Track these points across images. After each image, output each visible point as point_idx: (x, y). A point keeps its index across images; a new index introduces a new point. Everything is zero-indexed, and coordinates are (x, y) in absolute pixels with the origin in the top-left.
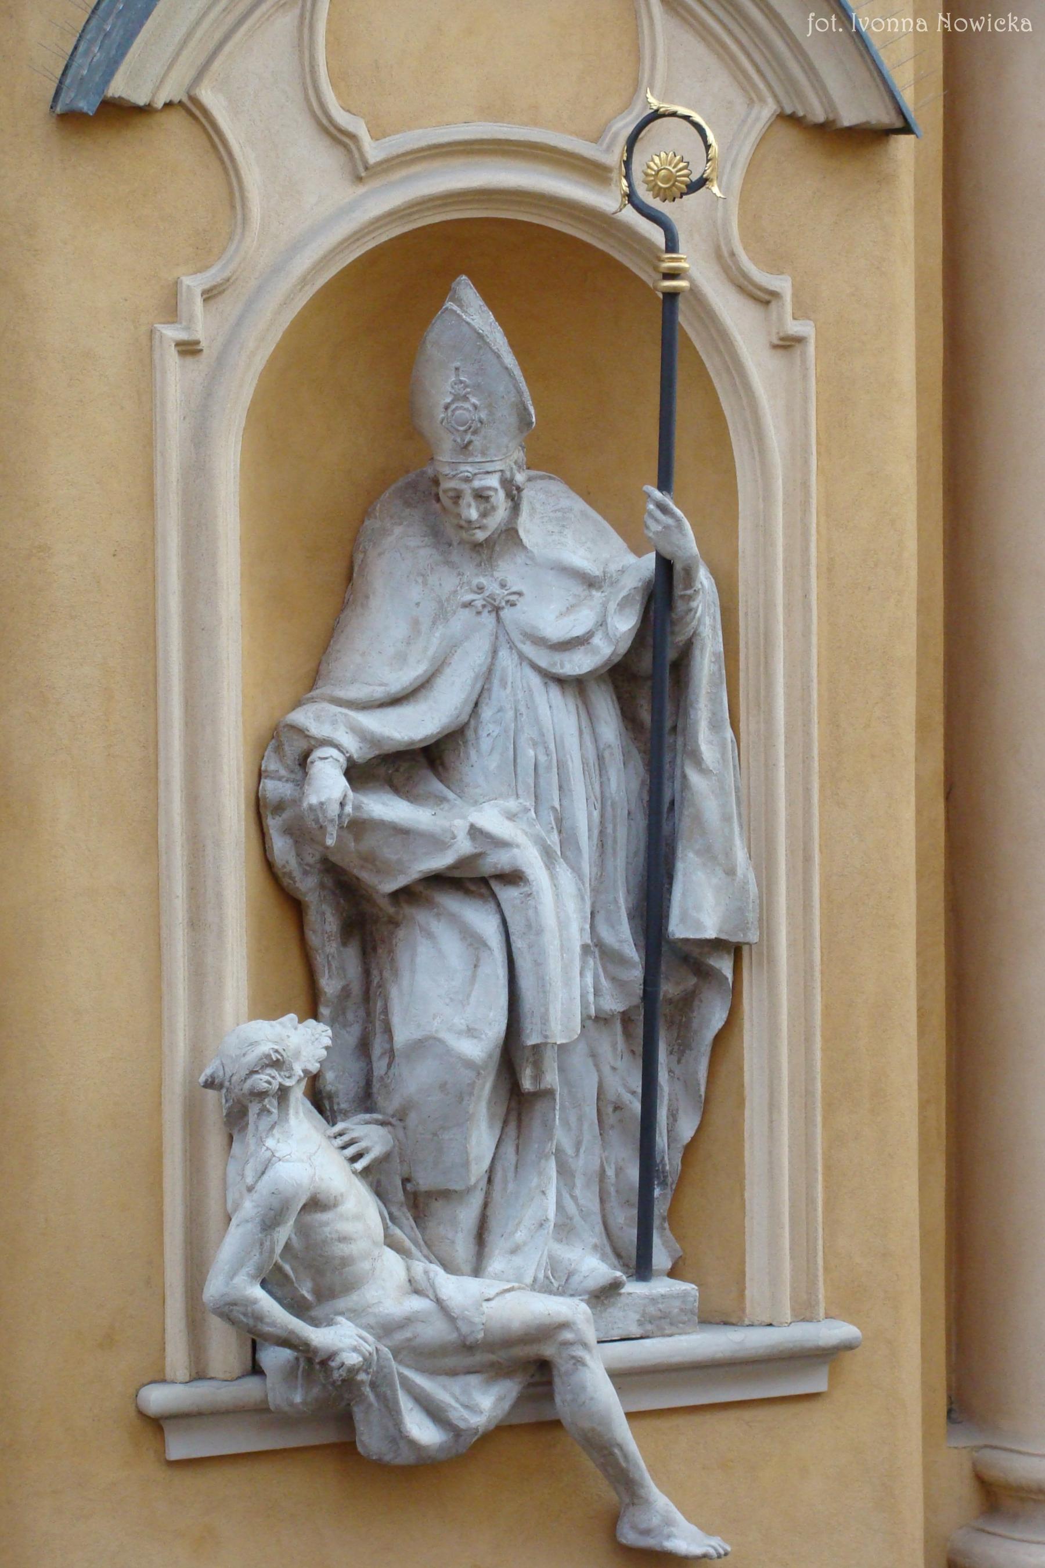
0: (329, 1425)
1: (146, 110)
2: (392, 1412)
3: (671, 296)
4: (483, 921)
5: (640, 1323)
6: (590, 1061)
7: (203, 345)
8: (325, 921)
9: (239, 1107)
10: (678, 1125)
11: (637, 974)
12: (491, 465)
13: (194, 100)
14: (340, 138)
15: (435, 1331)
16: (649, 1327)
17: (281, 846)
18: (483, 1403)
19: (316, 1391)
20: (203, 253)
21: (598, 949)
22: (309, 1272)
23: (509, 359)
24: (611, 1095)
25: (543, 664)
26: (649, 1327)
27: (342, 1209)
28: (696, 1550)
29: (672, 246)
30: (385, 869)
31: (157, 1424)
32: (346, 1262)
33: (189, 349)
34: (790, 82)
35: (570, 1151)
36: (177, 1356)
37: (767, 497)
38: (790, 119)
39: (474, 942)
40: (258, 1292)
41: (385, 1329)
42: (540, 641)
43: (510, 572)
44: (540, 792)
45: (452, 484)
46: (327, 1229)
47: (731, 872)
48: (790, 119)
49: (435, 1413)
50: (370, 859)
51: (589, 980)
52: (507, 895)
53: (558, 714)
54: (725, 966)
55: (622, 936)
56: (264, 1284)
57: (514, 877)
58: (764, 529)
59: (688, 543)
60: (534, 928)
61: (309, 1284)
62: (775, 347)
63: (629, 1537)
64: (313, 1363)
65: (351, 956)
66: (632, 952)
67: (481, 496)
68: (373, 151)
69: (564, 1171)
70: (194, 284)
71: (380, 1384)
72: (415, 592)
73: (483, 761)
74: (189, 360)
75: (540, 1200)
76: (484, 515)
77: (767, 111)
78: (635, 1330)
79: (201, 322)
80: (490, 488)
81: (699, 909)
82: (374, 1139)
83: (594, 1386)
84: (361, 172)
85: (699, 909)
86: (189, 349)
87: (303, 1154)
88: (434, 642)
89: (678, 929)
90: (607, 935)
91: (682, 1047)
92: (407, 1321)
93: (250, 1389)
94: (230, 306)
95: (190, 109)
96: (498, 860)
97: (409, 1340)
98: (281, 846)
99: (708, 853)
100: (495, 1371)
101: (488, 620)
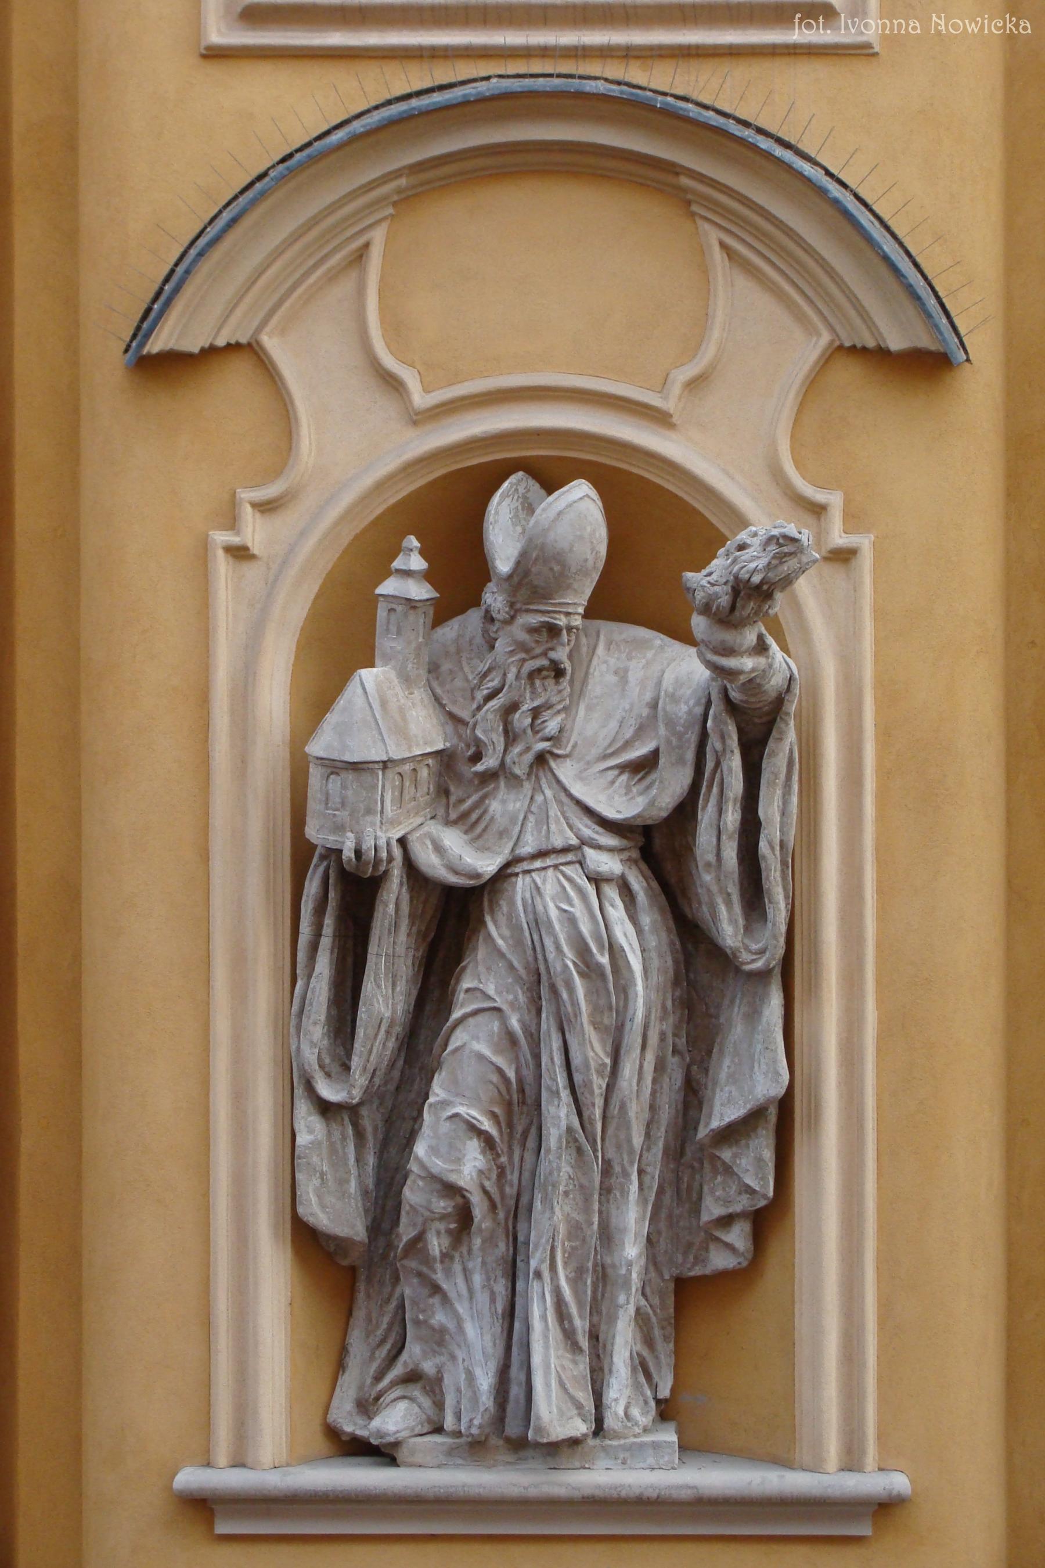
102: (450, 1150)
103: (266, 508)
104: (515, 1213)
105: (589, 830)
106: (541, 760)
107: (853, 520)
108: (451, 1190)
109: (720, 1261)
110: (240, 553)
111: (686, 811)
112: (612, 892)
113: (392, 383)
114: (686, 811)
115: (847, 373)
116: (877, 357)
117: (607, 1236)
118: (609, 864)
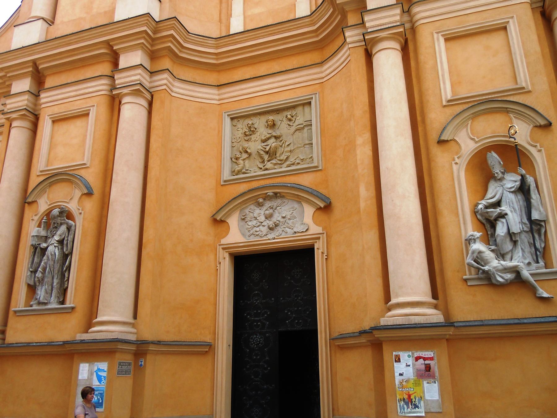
0: (487, 279)
1: (447, 141)
2: (495, 277)
3: (516, 145)
4: (504, 220)
8: (488, 226)
9: (469, 241)
11: (529, 225)
12: (497, 170)
15: (501, 267)
17: (479, 217)
18: (509, 276)
20: (457, 153)
21: (522, 223)
22: (479, 259)
23: (498, 158)
29: (515, 139)
30: (491, 217)
31: (466, 280)
32: (487, 260)
33: (456, 163)
34: (534, 122)
36: (467, 273)
37: (539, 167)
38: (536, 126)
39: (503, 223)
40: (473, 262)
41: (494, 268)
43: (504, 182)
44: (510, 204)
47: (540, 211)
48: (536, 126)
50: (489, 216)
51: (521, 226)
52: (506, 216)
53: (512, 196)
54: (543, 224)
55: (525, 220)
56: (474, 261)
57: (506, 214)
58: (539, 172)
59: (524, 172)
60: (509, 219)
63: (537, 295)
64: (484, 271)
65: (492, 230)
66: (527, 222)
67: (497, 173)
68: (477, 140)
69: (523, 250)
70: (456, 157)
71: (494, 274)
72: (493, 187)
73: (503, 203)
75: (518, 254)
77: (532, 126)
79: (457, 160)
81: (535, 215)
82: (493, 247)
83: (526, 273)
84: (476, 142)
85: (535, 215)
86: (456, 163)
87: (478, 246)
88: (495, 191)
89: (532, 219)
90: (523, 221)
91: (540, 235)
92: (497, 267)
93: (477, 276)
94: (461, 158)
95: (454, 140)
96: (504, 212)
98: (479, 217)
99: (536, 210)
102: (39, 275)
103: (36, 215)
104: (43, 279)
105: (55, 242)
106: (53, 236)
107: (82, 210)
108: (38, 278)
109: (66, 286)
110: (33, 220)
111: (64, 239)
112: (57, 248)
113: (47, 203)
114: (64, 239)
115: (84, 197)
116: (85, 194)
117: (53, 283)
118: (55, 245)
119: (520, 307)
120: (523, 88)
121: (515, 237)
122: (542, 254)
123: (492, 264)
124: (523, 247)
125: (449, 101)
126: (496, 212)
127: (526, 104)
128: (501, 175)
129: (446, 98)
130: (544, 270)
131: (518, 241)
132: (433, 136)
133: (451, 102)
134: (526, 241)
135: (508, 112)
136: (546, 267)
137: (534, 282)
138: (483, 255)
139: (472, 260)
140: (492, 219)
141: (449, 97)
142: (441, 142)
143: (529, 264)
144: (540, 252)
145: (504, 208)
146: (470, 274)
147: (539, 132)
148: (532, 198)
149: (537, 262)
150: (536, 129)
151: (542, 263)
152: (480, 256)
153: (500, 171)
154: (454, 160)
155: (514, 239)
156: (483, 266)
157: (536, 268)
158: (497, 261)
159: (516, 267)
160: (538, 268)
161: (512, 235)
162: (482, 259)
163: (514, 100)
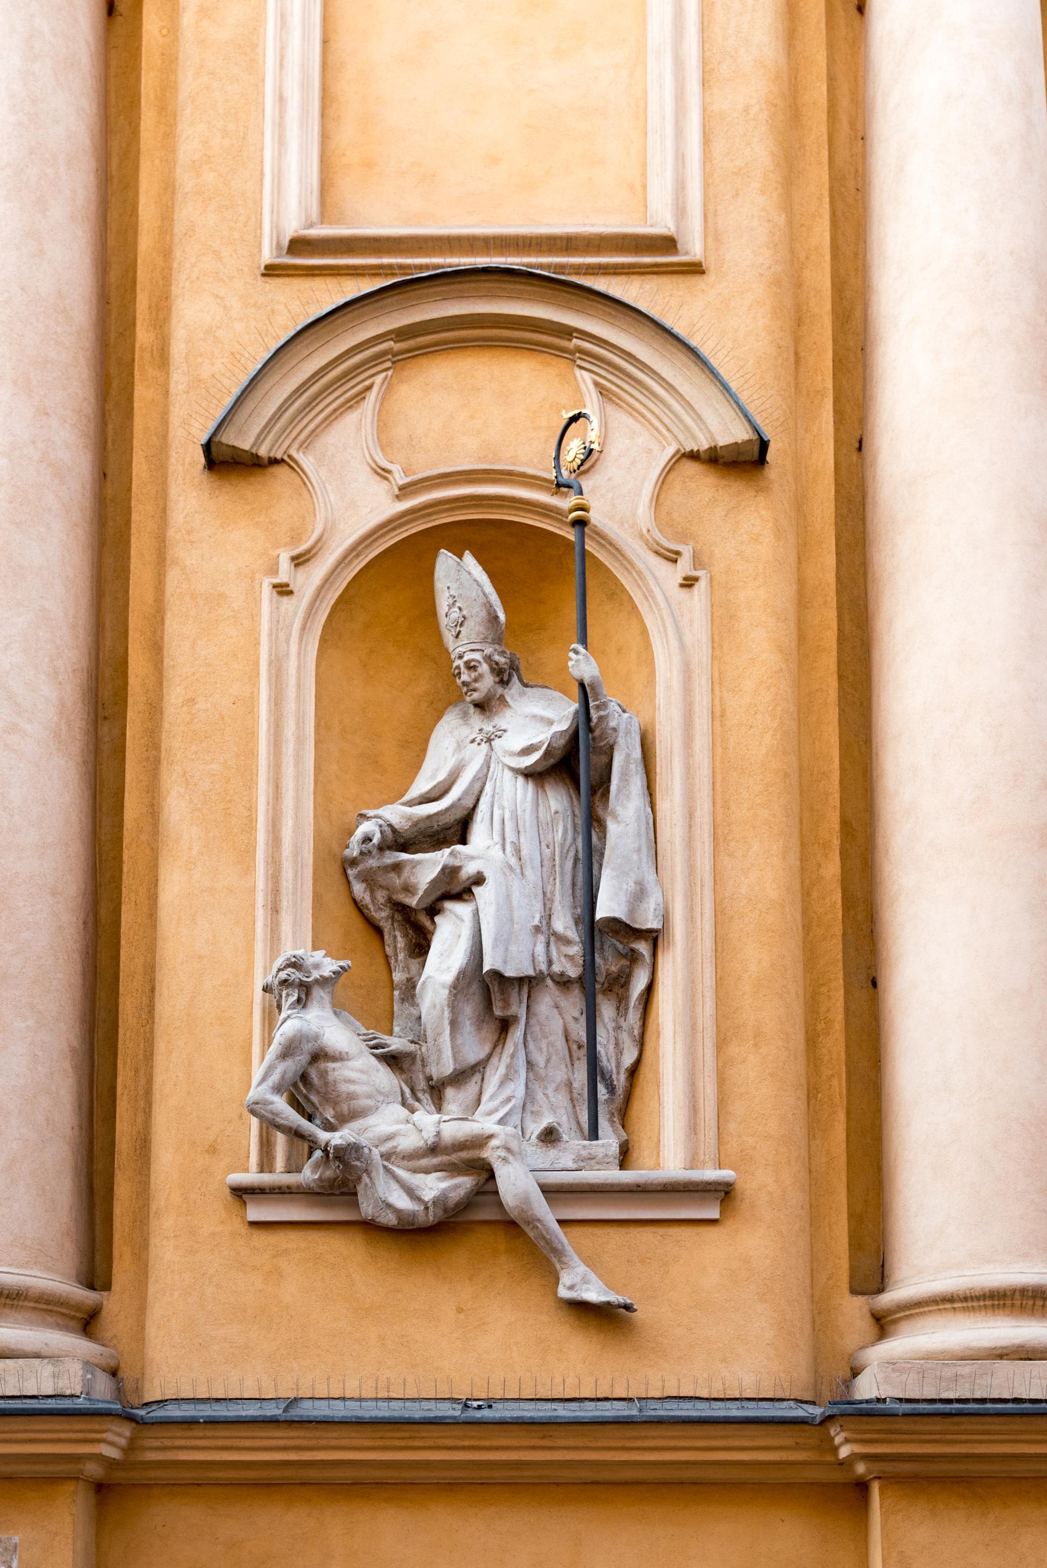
5: (575, 1161)
6: (555, 1011)
7: (291, 587)
10: (615, 1051)
13: (289, 456)
14: (383, 473)
16: (582, 1164)
19: (328, 1174)
24: (574, 1036)
25: (513, 765)
26: (582, 1164)
27: (350, 1064)
28: (603, 1298)
35: (542, 1064)
42: (512, 754)
45: (455, 665)
46: (336, 1073)
49: (410, 1192)
51: (540, 949)
54: (643, 947)
61: (332, 1112)
62: (682, 586)
66: (572, 934)
67: (470, 667)
74: (285, 599)
76: (476, 680)
78: (571, 1165)
80: (473, 660)
91: (622, 1002)
97: (395, 1147)
100: (452, 1169)
101: (485, 747)
119: (473, 1346)
120: (668, 244)
121: (507, 1004)
122: (612, 1095)
123: (370, 1120)
124: (540, 1059)
125: (298, 245)
126: (435, 863)
127: (668, 323)
128: (488, 682)
129: (276, 226)
130: (614, 1175)
131: (515, 1019)
132: (190, 425)
133: (303, 255)
134: (556, 1026)
135: (574, 356)
136: (623, 1165)
137: (556, 1226)
138: (338, 1071)
139: (278, 1089)
140: (413, 901)
141: (293, 227)
142: (223, 461)
143: (550, 1136)
144: (611, 1089)
145: (480, 851)
146: (266, 1164)
147: (702, 486)
148: (615, 817)
149: (594, 1134)
150: (691, 468)
151: (609, 1141)
152: (323, 1075)
153: (488, 659)
154: (274, 570)
155: (498, 1012)
156: (329, 1127)
157: (579, 1158)
158: (404, 1112)
159: (481, 1141)
160: (586, 1161)
161: (495, 988)
162: (331, 1097)
163: (626, 299)
